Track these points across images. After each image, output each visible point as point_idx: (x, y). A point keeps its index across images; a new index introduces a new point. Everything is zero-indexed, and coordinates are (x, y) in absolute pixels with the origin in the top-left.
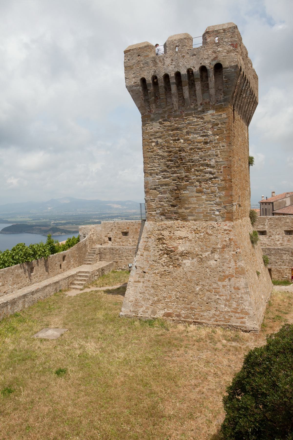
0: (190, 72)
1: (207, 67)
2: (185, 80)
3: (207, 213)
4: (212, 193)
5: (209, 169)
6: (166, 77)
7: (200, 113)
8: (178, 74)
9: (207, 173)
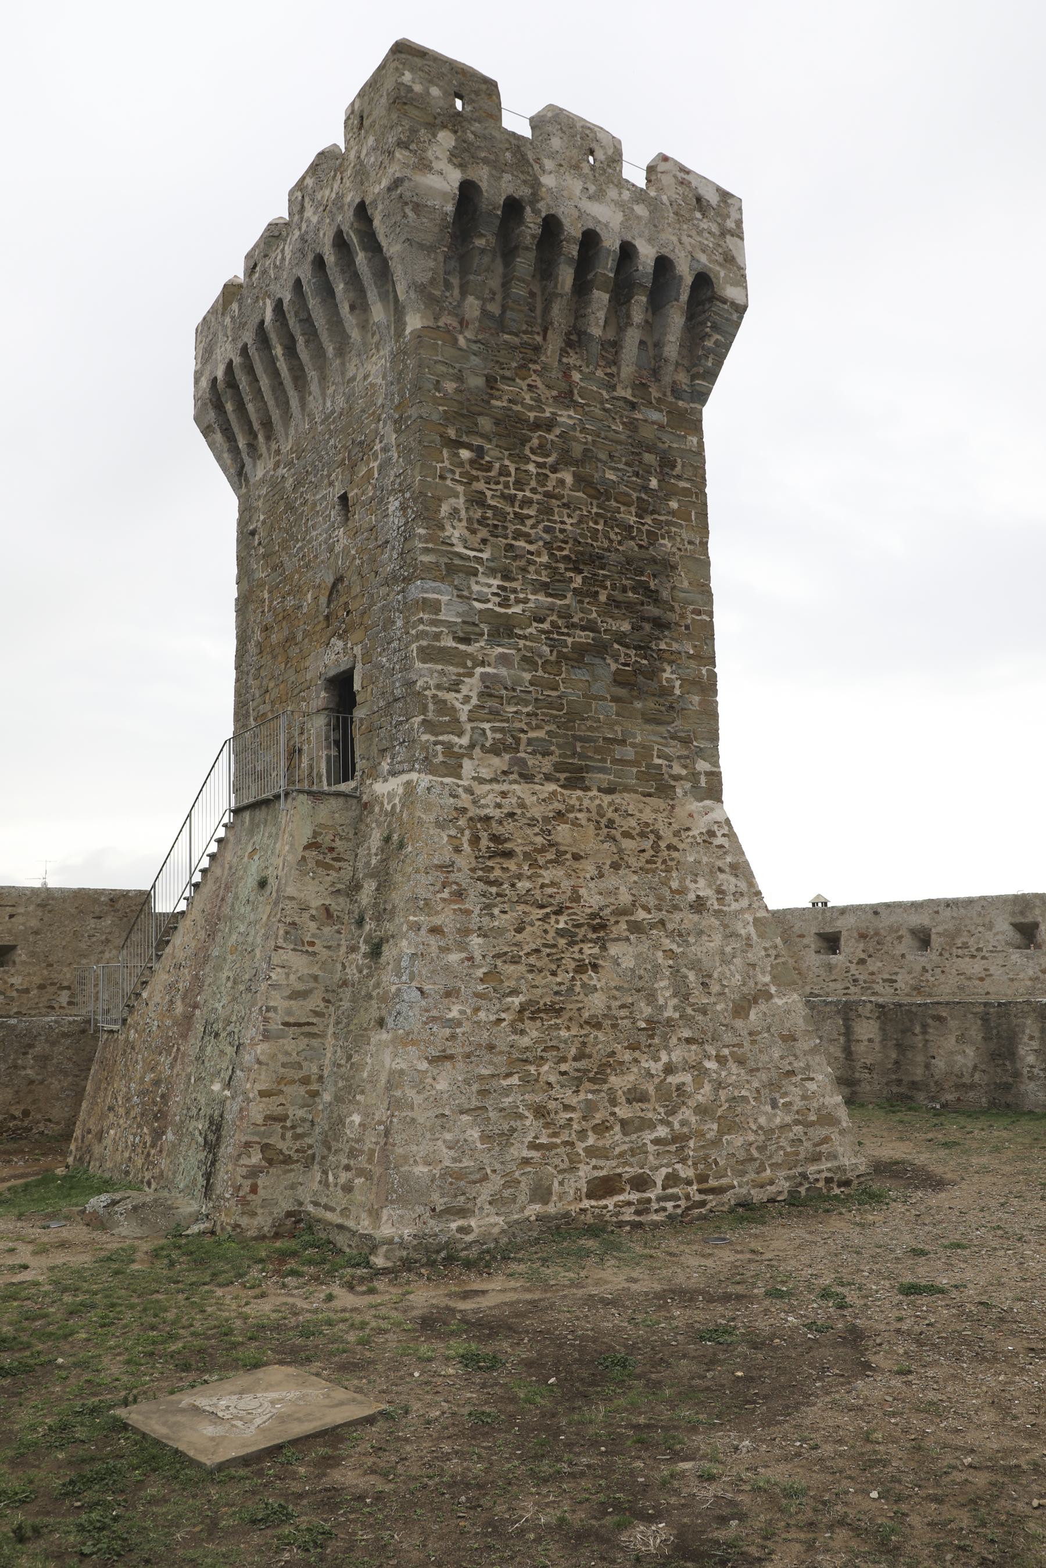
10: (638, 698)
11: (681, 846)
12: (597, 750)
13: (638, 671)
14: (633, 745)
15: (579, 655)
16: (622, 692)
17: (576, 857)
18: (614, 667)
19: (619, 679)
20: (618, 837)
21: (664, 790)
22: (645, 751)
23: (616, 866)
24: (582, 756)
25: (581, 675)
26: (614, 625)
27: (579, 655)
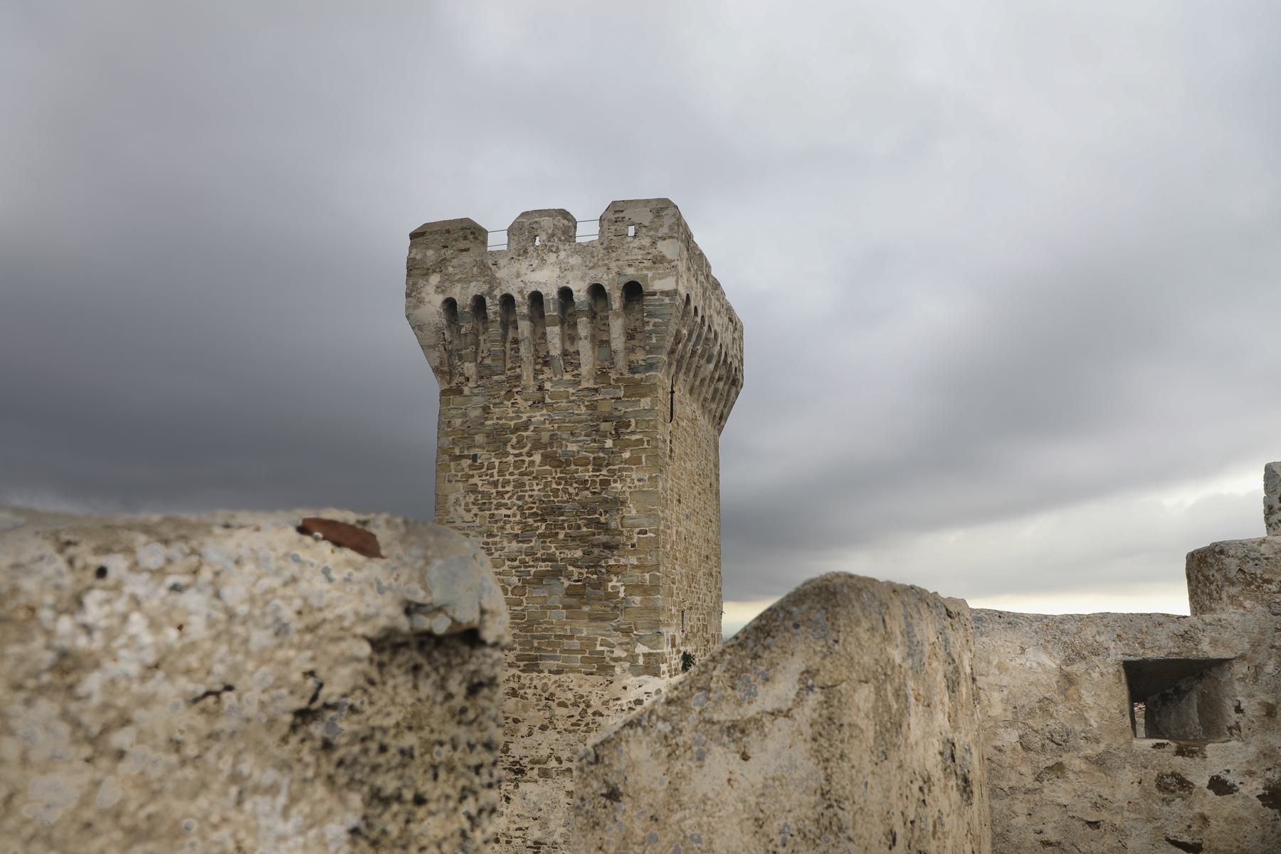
0: (566, 294)
1: (607, 288)
2: (551, 310)
3: (591, 653)
4: (607, 599)
5: (603, 538)
6: (508, 301)
7: (585, 393)
8: (536, 298)
9: (598, 546)
10: (586, 604)
11: (605, 712)
12: (549, 644)
13: (587, 583)
14: (578, 638)
15: (540, 578)
16: (573, 601)
17: (516, 721)
18: (567, 583)
19: (570, 592)
20: (553, 705)
21: (603, 667)
22: (592, 641)
23: (543, 728)
24: (538, 649)
25: (541, 593)
26: (569, 554)
27: (540, 578)
